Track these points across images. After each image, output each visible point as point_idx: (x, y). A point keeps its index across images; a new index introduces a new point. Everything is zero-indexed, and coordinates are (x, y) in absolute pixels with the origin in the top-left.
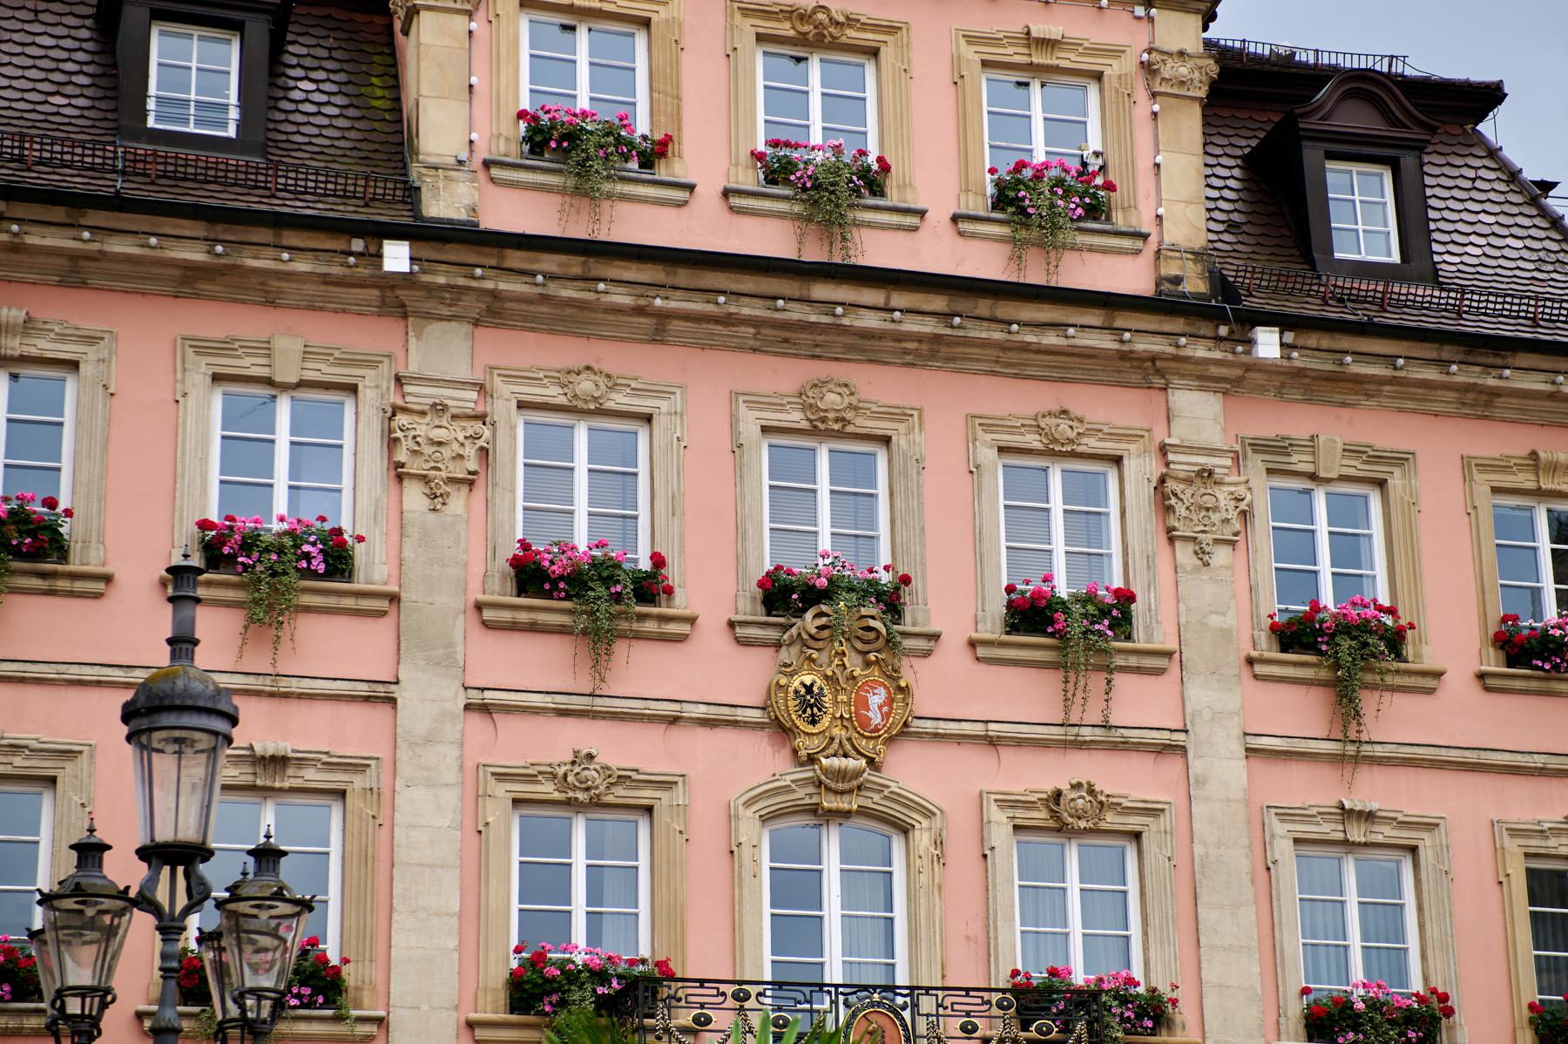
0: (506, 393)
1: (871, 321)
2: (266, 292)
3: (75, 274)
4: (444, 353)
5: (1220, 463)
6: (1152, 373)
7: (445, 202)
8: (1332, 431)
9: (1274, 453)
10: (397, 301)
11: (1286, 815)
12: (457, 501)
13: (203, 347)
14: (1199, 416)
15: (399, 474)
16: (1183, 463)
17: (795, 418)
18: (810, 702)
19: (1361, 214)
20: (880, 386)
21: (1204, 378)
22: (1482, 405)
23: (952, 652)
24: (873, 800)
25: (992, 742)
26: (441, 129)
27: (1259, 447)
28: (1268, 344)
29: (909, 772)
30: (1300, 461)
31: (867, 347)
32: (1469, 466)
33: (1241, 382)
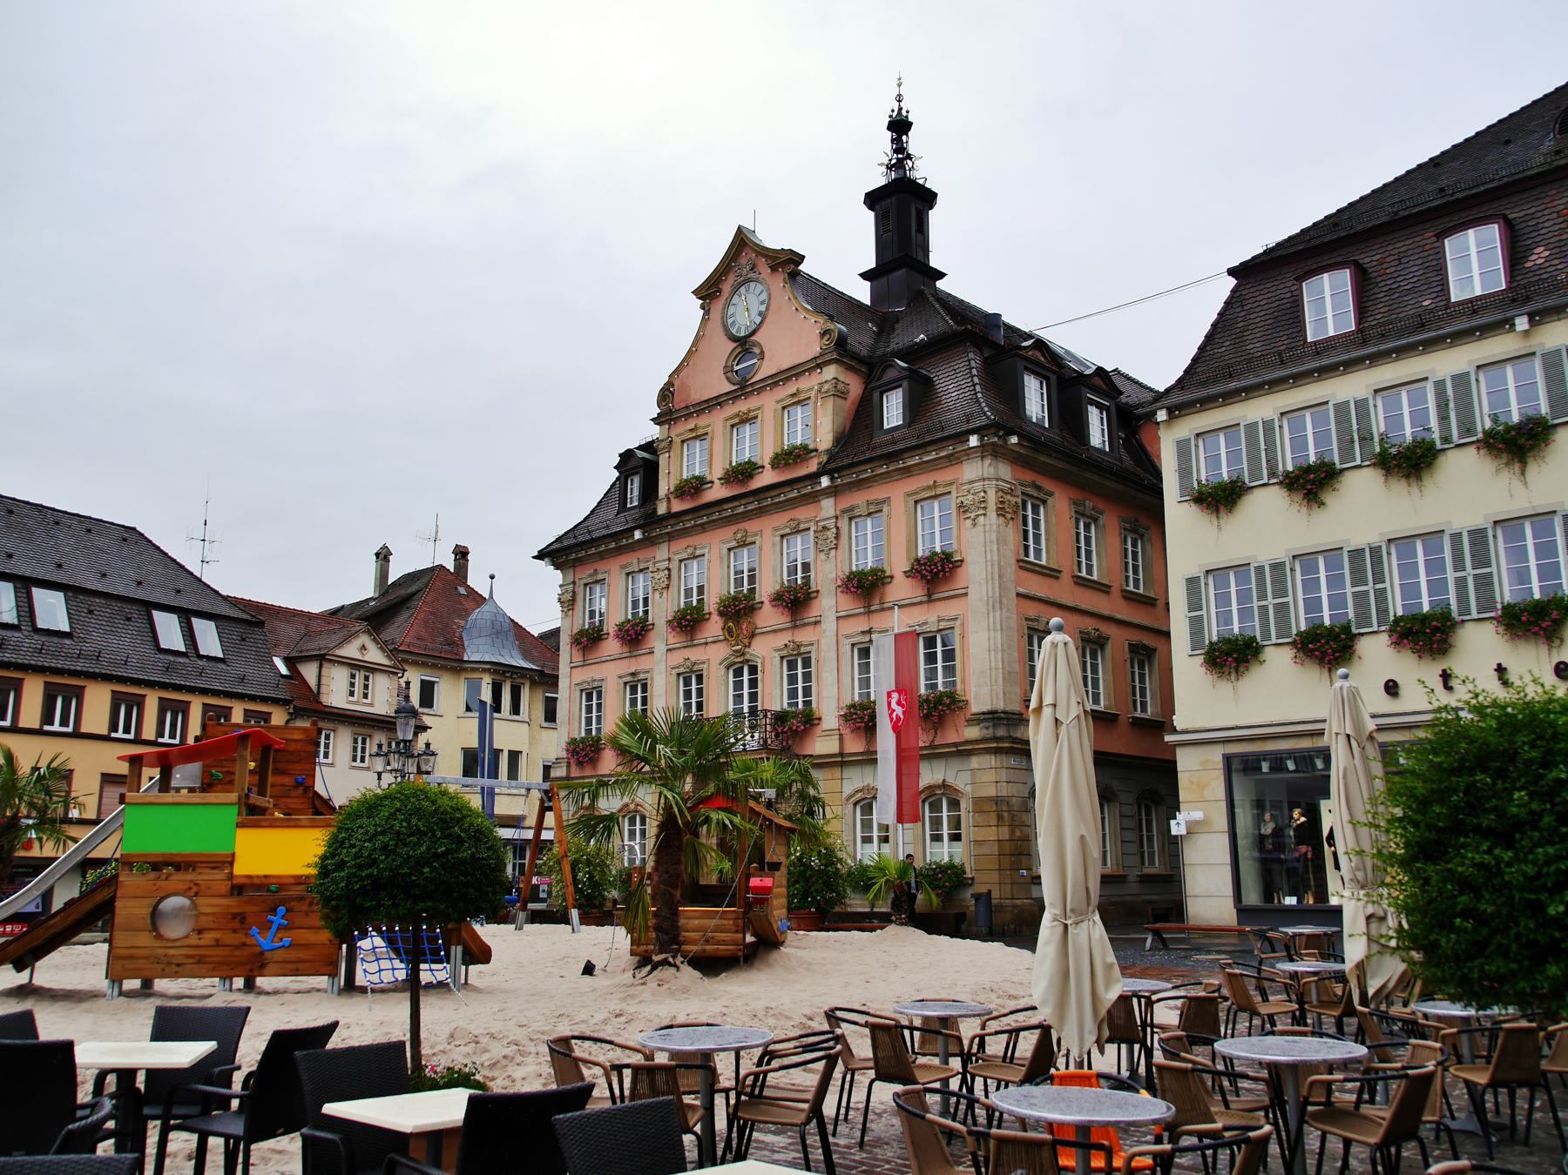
1: (741, 509)
5: (831, 523)
8: (859, 499)
10: (649, 542)
11: (847, 637)
13: (623, 567)
14: (828, 507)
17: (734, 544)
20: (752, 526)
22: (907, 472)
23: (767, 607)
24: (747, 657)
25: (775, 631)
27: (844, 512)
28: (825, 481)
30: (857, 512)
31: (747, 516)
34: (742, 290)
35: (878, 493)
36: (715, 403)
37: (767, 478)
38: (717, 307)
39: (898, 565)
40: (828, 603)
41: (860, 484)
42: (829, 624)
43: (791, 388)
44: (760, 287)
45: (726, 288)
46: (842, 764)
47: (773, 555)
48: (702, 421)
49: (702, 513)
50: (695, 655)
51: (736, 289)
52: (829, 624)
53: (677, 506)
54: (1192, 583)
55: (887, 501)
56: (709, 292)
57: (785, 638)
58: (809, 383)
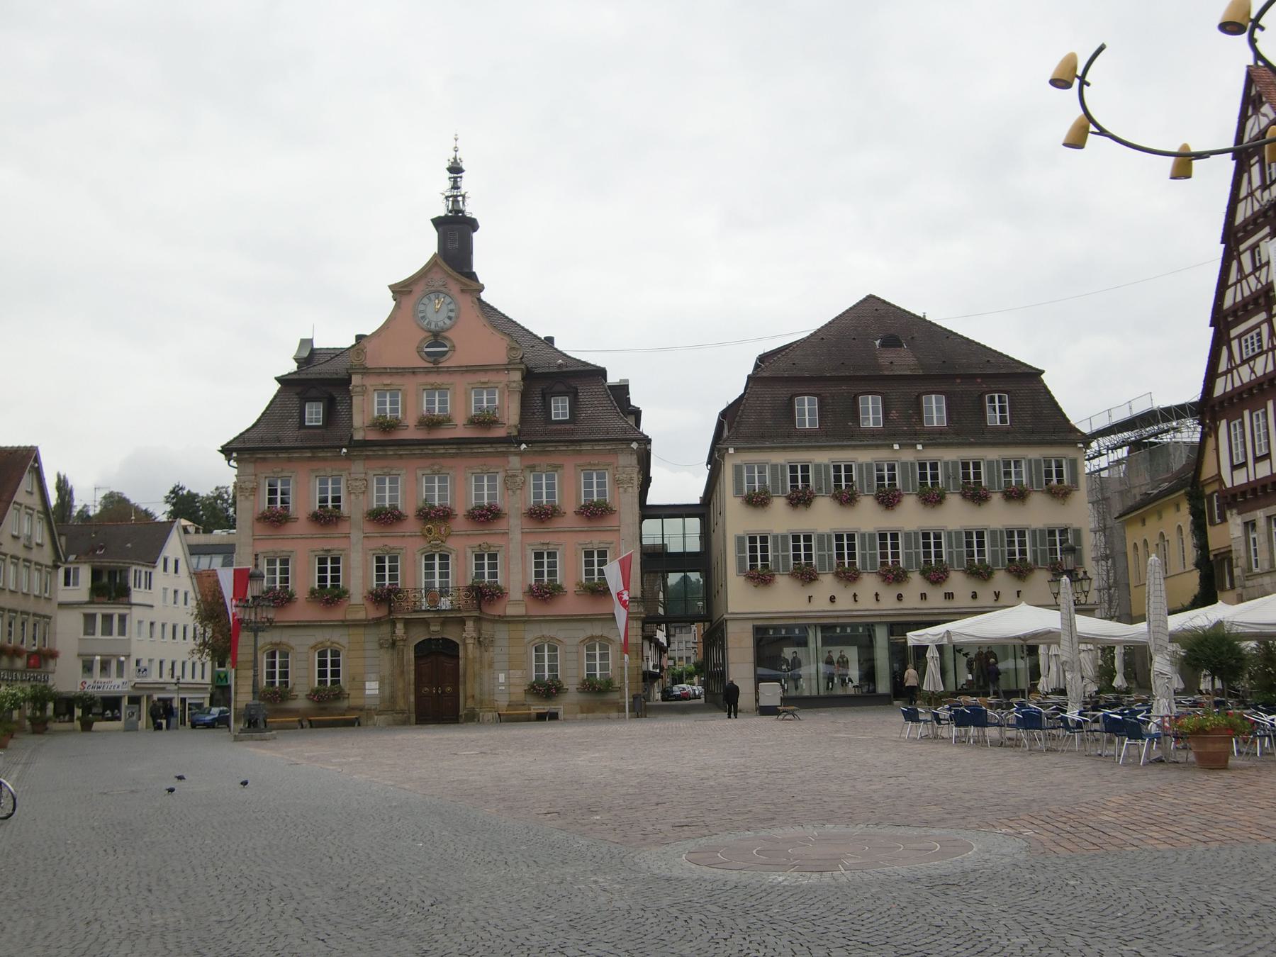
0: (371, 473)
2: (325, 459)
3: (290, 460)
4: (358, 467)
6: (505, 454)
7: (358, 436)
8: (542, 461)
9: (532, 468)
12: (361, 497)
13: (313, 471)
14: (515, 462)
15: (350, 493)
16: (510, 473)
18: (429, 531)
19: (560, 408)
21: (516, 454)
26: (358, 421)
29: (452, 544)
32: (576, 466)
33: (521, 454)
34: (432, 296)
35: (556, 460)
36: (414, 371)
37: (460, 433)
38: (408, 301)
39: (570, 507)
40: (515, 523)
41: (544, 452)
42: (516, 536)
43: (484, 378)
44: (448, 300)
45: (419, 289)
46: (525, 622)
47: (464, 487)
48: (397, 381)
49: (387, 443)
50: (391, 543)
51: (427, 295)
52: (516, 536)
53: (373, 436)
54: (740, 540)
55: (561, 466)
56: (400, 291)
57: (476, 542)
58: (502, 378)
